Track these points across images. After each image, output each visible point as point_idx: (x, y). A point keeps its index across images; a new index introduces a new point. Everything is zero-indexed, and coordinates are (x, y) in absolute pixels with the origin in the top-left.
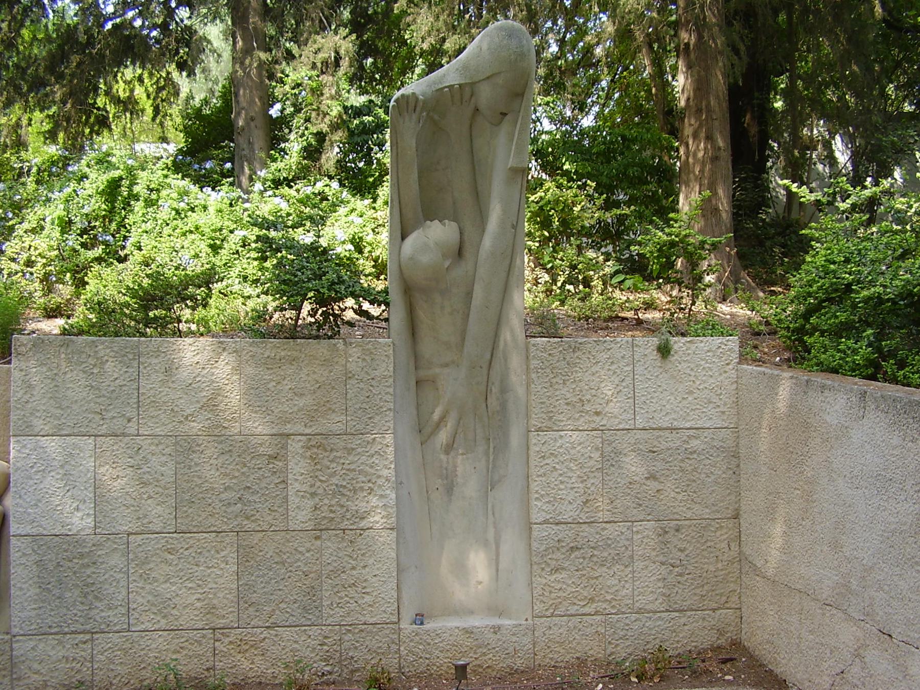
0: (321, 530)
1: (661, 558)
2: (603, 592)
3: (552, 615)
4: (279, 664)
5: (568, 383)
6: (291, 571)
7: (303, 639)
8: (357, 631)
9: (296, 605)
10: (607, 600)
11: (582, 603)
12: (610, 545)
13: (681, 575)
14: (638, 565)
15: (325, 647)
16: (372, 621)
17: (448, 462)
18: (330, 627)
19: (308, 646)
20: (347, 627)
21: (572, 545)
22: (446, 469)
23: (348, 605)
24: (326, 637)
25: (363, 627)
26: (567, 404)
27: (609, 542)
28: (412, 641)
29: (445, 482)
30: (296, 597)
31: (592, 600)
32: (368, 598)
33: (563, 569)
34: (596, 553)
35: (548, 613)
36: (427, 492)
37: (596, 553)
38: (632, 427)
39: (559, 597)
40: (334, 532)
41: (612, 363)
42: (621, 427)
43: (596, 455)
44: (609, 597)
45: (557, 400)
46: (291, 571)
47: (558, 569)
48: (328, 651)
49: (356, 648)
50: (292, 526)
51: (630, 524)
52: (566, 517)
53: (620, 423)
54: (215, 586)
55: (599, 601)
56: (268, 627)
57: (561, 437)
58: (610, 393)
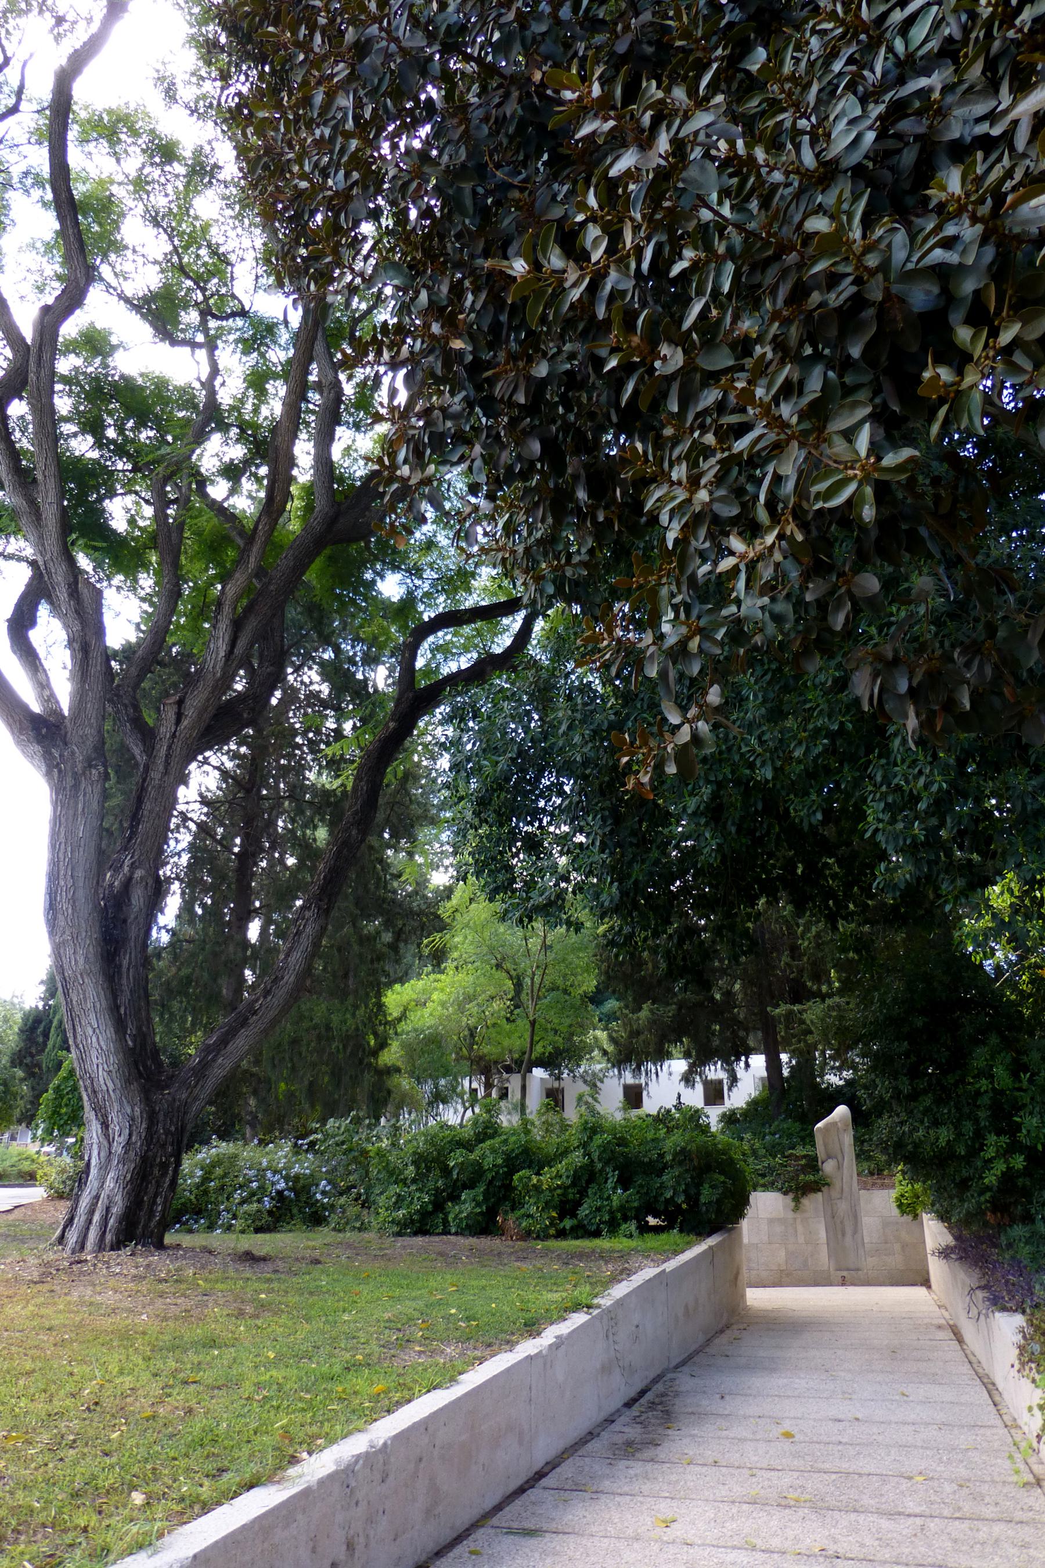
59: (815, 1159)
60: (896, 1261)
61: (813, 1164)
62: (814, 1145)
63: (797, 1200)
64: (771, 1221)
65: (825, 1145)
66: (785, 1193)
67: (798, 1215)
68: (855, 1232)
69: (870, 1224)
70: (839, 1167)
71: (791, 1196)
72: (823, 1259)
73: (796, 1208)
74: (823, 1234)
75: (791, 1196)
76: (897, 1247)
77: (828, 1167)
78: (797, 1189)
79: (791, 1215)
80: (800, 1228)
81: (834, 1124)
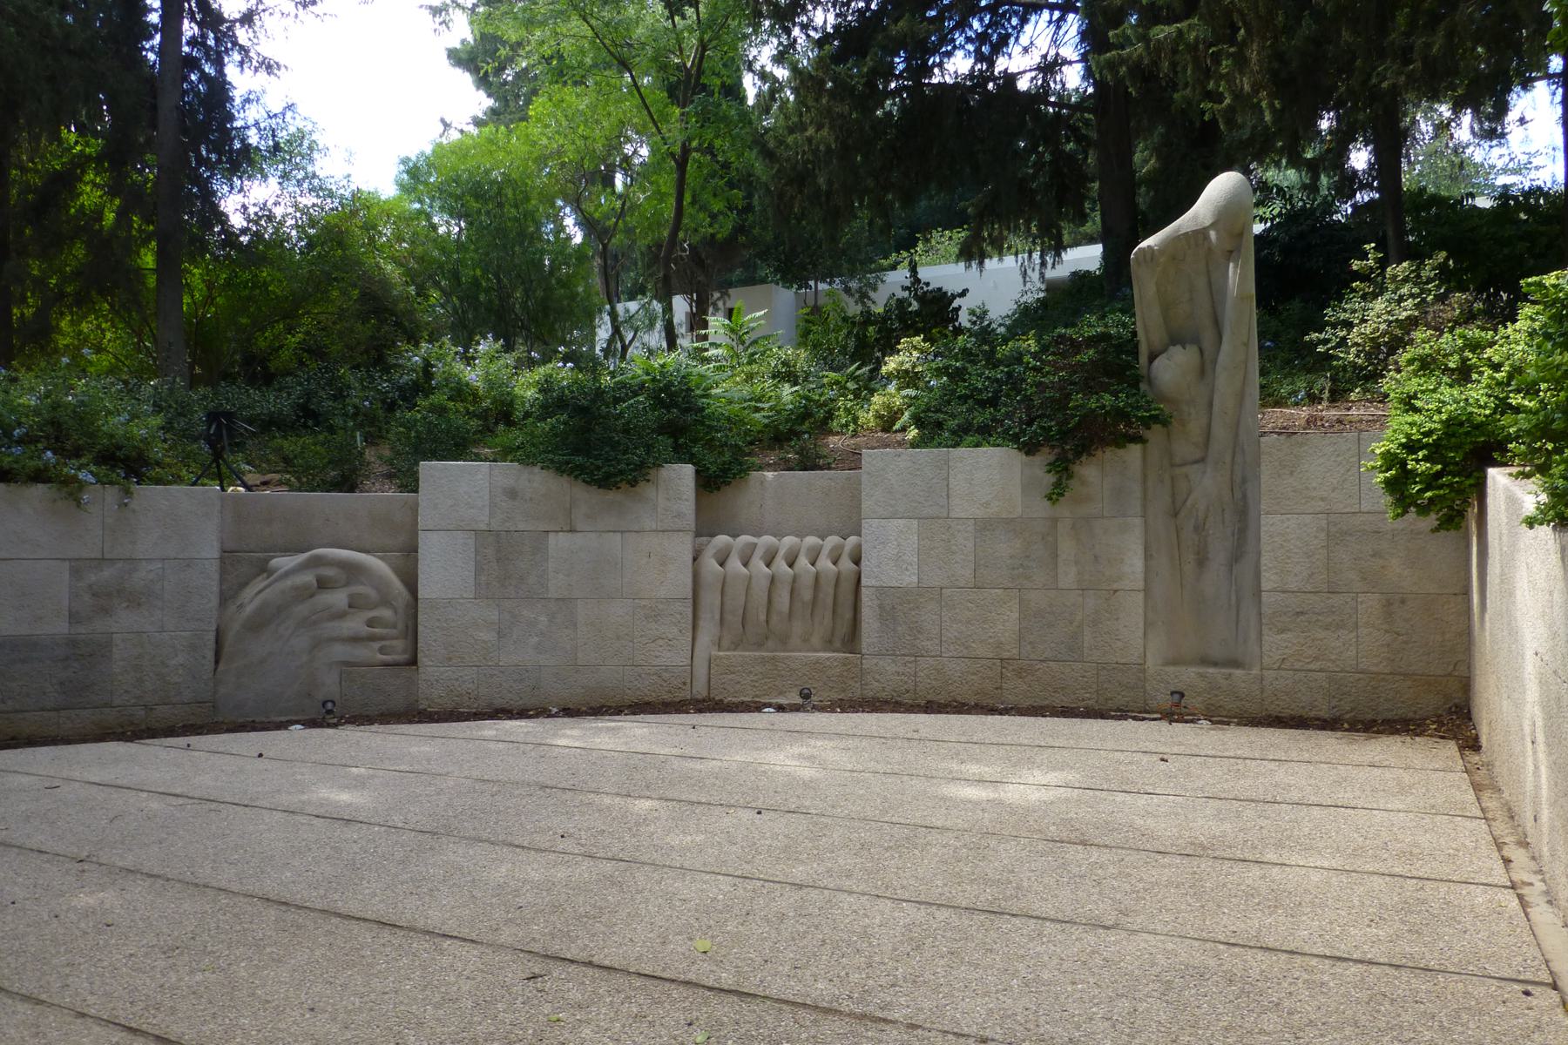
1: (1385, 627)
13: (1406, 643)
14: (1363, 631)
31: (1316, 659)
32: (1119, 644)
43: (1323, 535)
50: (1061, 585)
52: (1293, 587)
59: (1129, 345)
60: (1358, 648)
61: (1120, 363)
62: (1129, 310)
63: (1062, 469)
64: (984, 526)
65: (1166, 308)
66: (1029, 449)
67: (1064, 510)
68: (1236, 556)
69: (1286, 538)
70: (1205, 370)
71: (1044, 457)
72: (1132, 637)
73: (1056, 494)
74: (1134, 564)
75: (1044, 457)
76: (1370, 604)
77: (1171, 370)
78: (1065, 435)
79: (1042, 508)
80: (1067, 547)
81: (1200, 234)
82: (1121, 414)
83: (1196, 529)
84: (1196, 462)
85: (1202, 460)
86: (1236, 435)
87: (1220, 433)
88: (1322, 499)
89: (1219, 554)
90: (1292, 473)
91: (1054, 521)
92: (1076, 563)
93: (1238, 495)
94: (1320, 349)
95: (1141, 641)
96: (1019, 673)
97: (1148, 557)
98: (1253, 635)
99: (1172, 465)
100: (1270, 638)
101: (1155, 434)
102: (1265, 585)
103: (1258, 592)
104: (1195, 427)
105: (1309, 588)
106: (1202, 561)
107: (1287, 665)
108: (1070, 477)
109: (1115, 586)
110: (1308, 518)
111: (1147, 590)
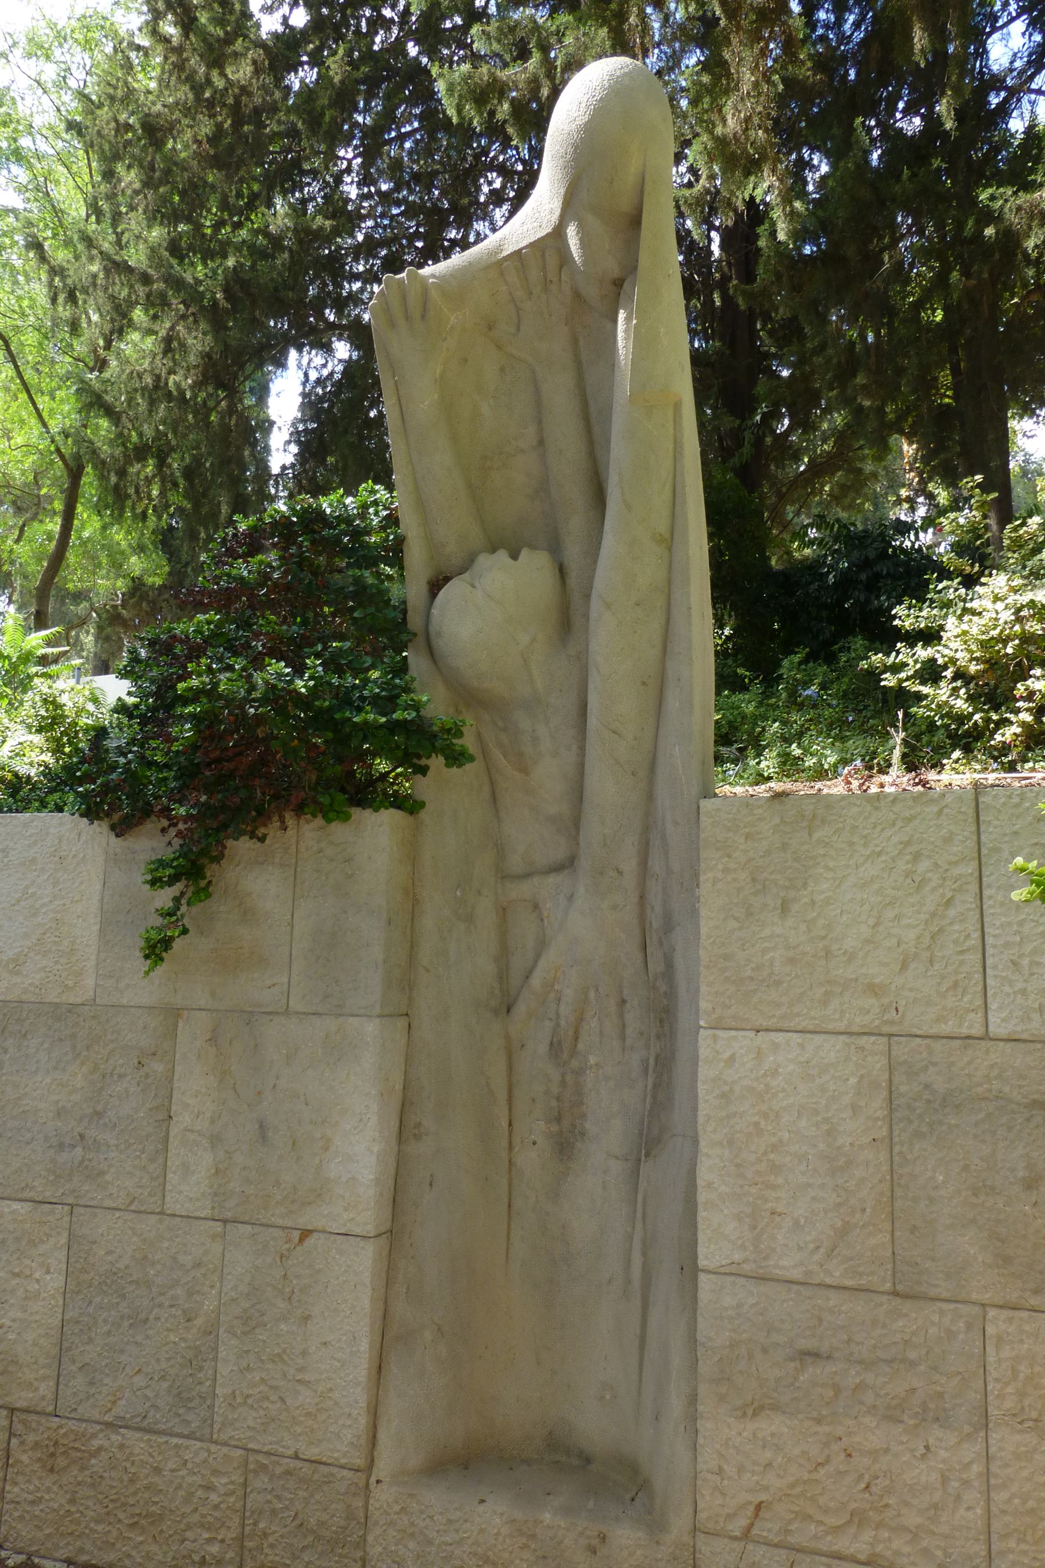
0: (225, 1222)
2: (892, 1501)
3: (746, 1535)
4: (122, 1516)
5: (795, 907)
6: (160, 1306)
7: (171, 1465)
8: (278, 1470)
9: (165, 1385)
10: (906, 1529)
11: (832, 1521)
12: (913, 1364)
14: (1005, 1440)
15: (214, 1498)
16: (312, 1453)
17: (563, 1083)
18: (225, 1450)
19: (179, 1487)
20: (261, 1458)
21: (803, 1344)
22: (558, 1099)
23: (265, 1404)
24: (216, 1472)
25: (293, 1464)
26: (791, 961)
27: (912, 1355)
28: (392, 1523)
29: (555, 1128)
30: (164, 1365)
31: (858, 1519)
33: (775, 1407)
34: (869, 1378)
35: (737, 1527)
36: (511, 1147)
37: (869, 1378)
38: (977, 1030)
39: (766, 1488)
40: (249, 1227)
41: (917, 857)
42: (946, 1029)
44: (912, 1520)
45: (765, 951)
46: (160, 1306)
47: (762, 1408)
48: (216, 1507)
49: (274, 1512)
51: (977, 1309)
53: (940, 1019)
54: (19, 1315)
55: (879, 1525)
56: (108, 1425)
57: (776, 1046)
58: (912, 934)
63: (191, 871)
74: (357, 1156)
77: (480, 619)
80: (194, 1093)
82: (325, 715)
83: (555, 1047)
84: (557, 868)
85: (567, 865)
86: (650, 797)
87: (608, 789)
88: (874, 989)
89: (608, 1131)
90: (784, 909)
91: (173, 1014)
92: (215, 1140)
93: (656, 965)
94: (889, 681)
95: (359, 1398)
96: (53, 1457)
97: (405, 1130)
98: (676, 1405)
99: (504, 876)
100: (722, 1433)
101: (439, 785)
102: (708, 1255)
103: (689, 1270)
104: (549, 775)
105: (837, 1274)
106: (566, 1144)
107: (767, 1528)
108: (204, 893)
109: (306, 1219)
110: (831, 1048)
111: (394, 1235)
